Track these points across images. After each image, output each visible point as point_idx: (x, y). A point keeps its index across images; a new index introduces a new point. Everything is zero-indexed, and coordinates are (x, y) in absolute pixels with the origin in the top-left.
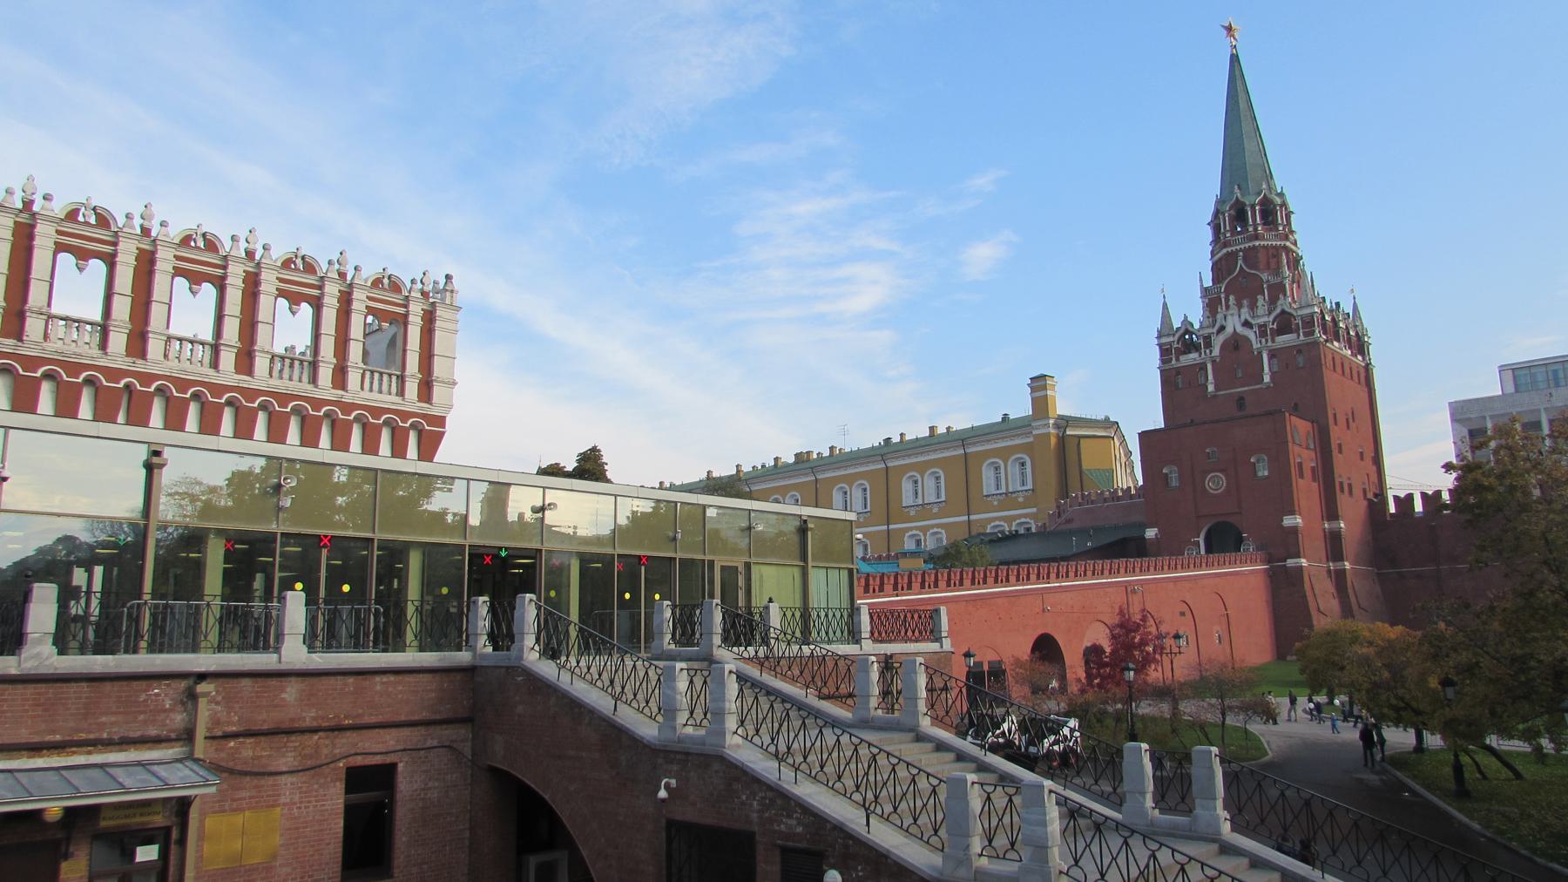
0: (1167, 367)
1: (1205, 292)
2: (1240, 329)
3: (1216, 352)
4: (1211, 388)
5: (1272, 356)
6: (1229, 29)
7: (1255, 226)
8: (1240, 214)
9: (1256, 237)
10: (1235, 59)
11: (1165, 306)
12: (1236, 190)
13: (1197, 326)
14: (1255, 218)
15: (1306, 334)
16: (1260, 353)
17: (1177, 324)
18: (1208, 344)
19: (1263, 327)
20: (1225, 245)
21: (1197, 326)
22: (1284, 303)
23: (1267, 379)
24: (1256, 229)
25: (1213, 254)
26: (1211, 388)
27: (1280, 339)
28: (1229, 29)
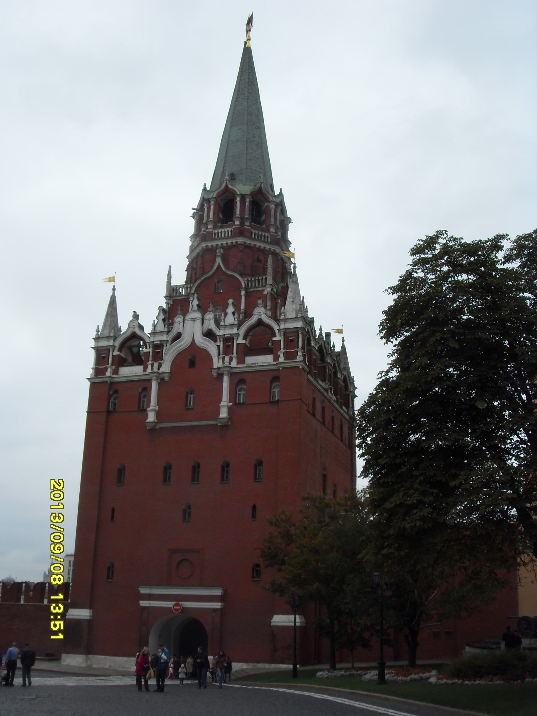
1: (172, 292)
2: (201, 341)
3: (166, 368)
4: (151, 417)
5: (239, 380)
6: (250, 21)
13: (148, 329)
16: (220, 376)
17: (124, 323)
18: (158, 356)
19: (228, 340)
21: (148, 329)
22: (261, 313)
23: (224, 414)
26: (151, 417)
27: (250, 360)
28: (250, 21)
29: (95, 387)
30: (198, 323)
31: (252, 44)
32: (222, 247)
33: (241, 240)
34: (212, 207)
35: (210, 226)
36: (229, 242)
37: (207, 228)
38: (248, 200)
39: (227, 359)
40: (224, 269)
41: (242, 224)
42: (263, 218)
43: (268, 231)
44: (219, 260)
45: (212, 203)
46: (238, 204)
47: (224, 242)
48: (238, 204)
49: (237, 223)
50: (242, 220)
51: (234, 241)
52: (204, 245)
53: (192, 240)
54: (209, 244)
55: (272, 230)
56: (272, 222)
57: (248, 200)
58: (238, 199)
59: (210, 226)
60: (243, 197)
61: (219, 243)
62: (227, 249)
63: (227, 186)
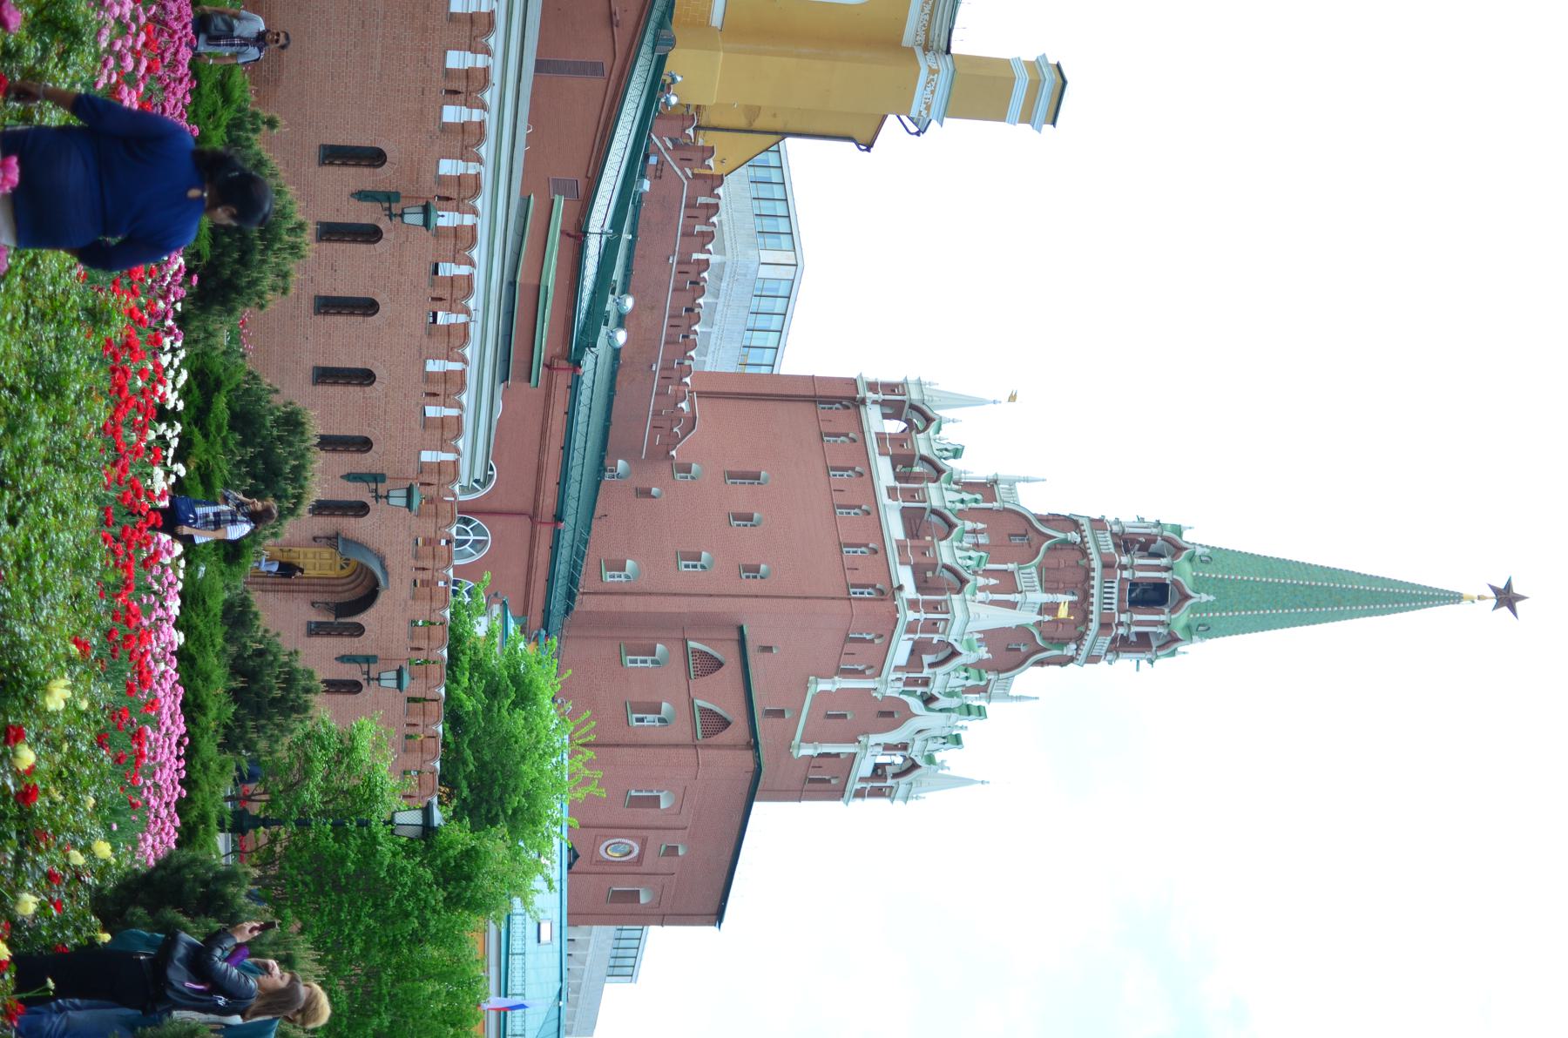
8: (1153, 595)
9: (1105, 626)
10: (1454, 598)
12: (1205, 597)
20: (1108, 565)
24: (1120, 624)
25: (1098, 524)
31: (1465, 605)
33: (1094, 626)
35: (1126, 574)
36: (1094, 608)
37: (1123, 567)
38: (1160, 630)
41: (1120, 624)
42: (1133, 638)
43: (1109, 651)
45: (1164, 575)
49: (1124, 617)
51: (1095, 617)
52: (1096, 564)
53: (1116, 528)
54: (1097, 574)
57: (1160, 630)
58: (1162, 618)
59: (1126, 574)
63: (1188, 597)
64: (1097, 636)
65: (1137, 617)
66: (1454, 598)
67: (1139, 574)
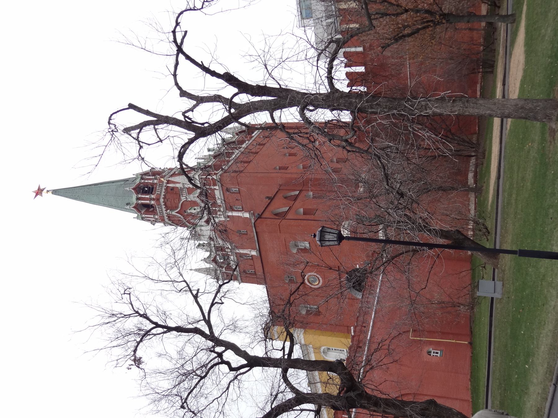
0: (239, 278)
7: (151, 199)
9: (158, 200)
10: (56, 192)
11: (196, 270)
14: (147, 199)
15: (215, 185)
16: (228, 217)
18: (222, 249)
23: (247, 215)
24: (153, 199)
29: (243, 282)
30: (202, 228)
32: (166, 210)
34: (146, 216)
35: (157, 217)
36: (163, 207)
38: (140, 196)
39: (219, 213)
40: (179, 209)
41: (153, 199)
44: (174, 213)
45: (144, 216)
46: (143, 202)
47: (164, 209)
48: (143, 202)
49: (153, 202)
50: (151, 199)
52: (167, 220)
55: (156, 181)
56: (151, 181)
58: (140, 202)
59: (157, 217)
60: (138, 199)
61: (165, 212)
62: (167, 208)
64: (160, 194)
65: (148, 202)
66: (56, 192)
67: (152, 216)
